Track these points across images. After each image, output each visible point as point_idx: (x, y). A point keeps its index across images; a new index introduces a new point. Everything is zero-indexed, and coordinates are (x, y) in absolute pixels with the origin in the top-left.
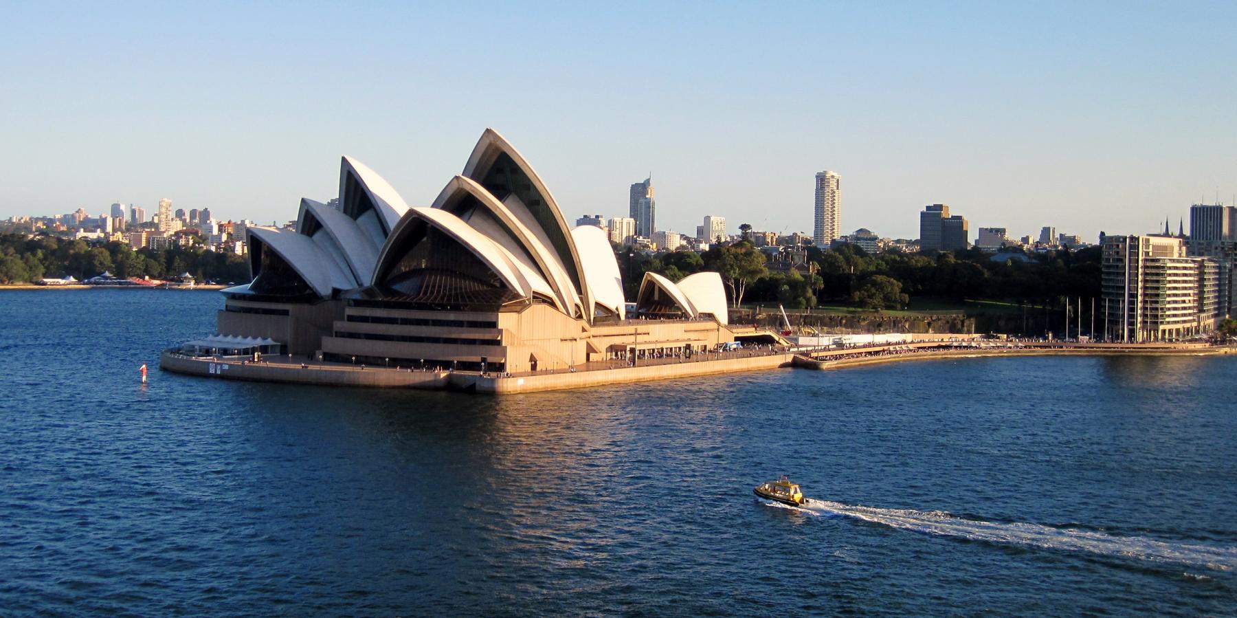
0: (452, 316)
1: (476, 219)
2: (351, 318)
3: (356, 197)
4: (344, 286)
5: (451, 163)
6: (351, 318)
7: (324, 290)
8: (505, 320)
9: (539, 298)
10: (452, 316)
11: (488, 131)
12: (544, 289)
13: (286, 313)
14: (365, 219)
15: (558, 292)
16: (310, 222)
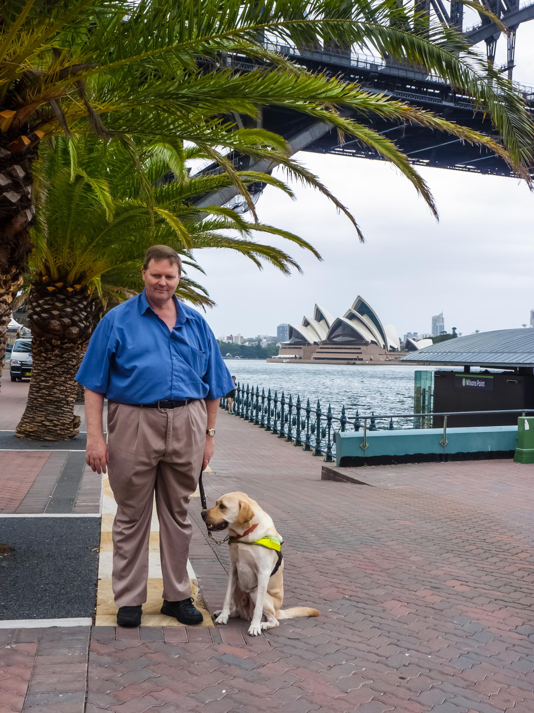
0: (349, 347)
1: (355, 321)
2: (321, 348)
3: (320, 316)
4: (317, 341)
5: (349, 305)
6: (321, 348)
7: (312, 342)
8: (363, 348)
9: (373, 342)
10: (349, 347)
11: (359, 296)
12: (374, 340)
13: (301, 348)
14: (322, 322)
15: (378, 341)
16: (306, 324)
